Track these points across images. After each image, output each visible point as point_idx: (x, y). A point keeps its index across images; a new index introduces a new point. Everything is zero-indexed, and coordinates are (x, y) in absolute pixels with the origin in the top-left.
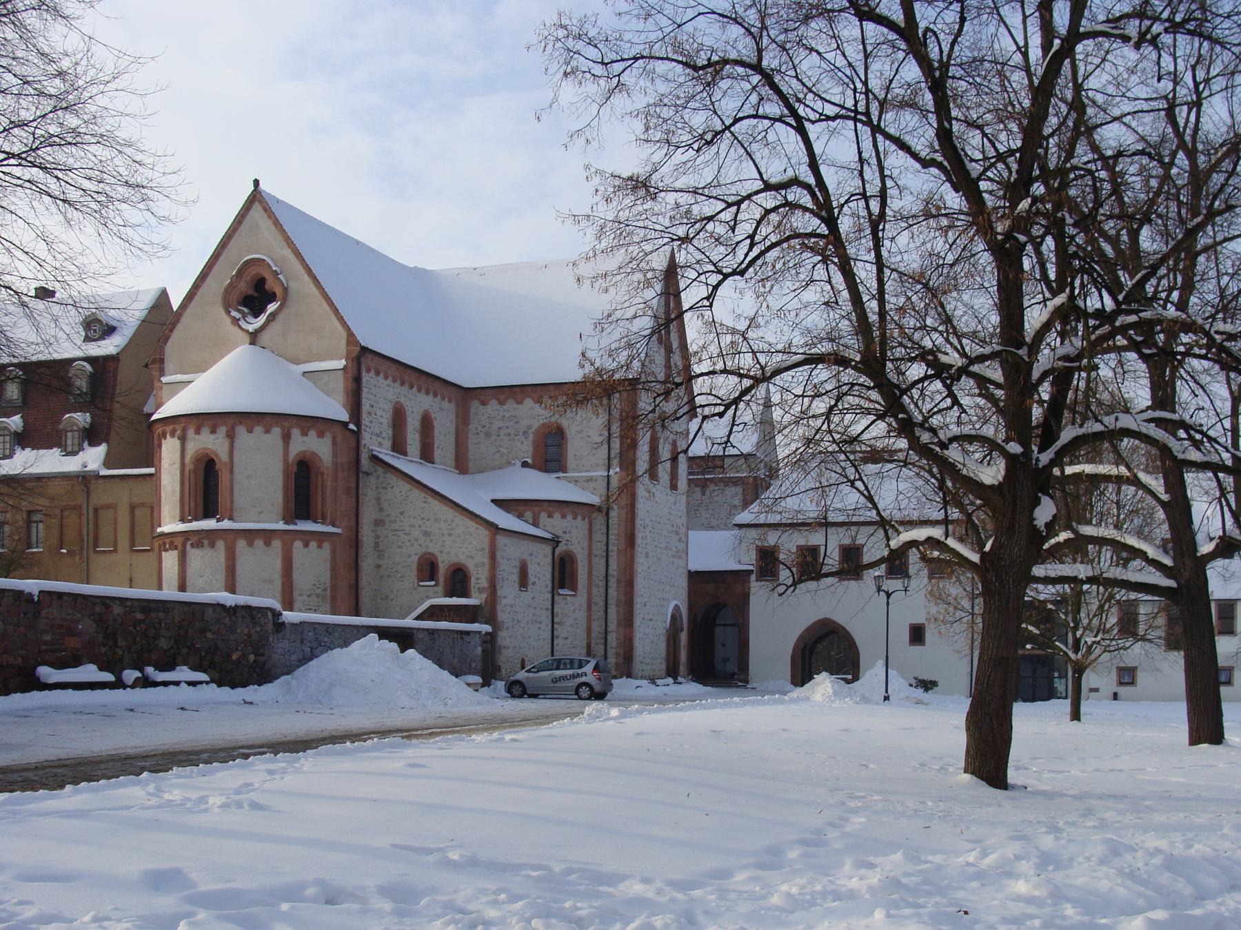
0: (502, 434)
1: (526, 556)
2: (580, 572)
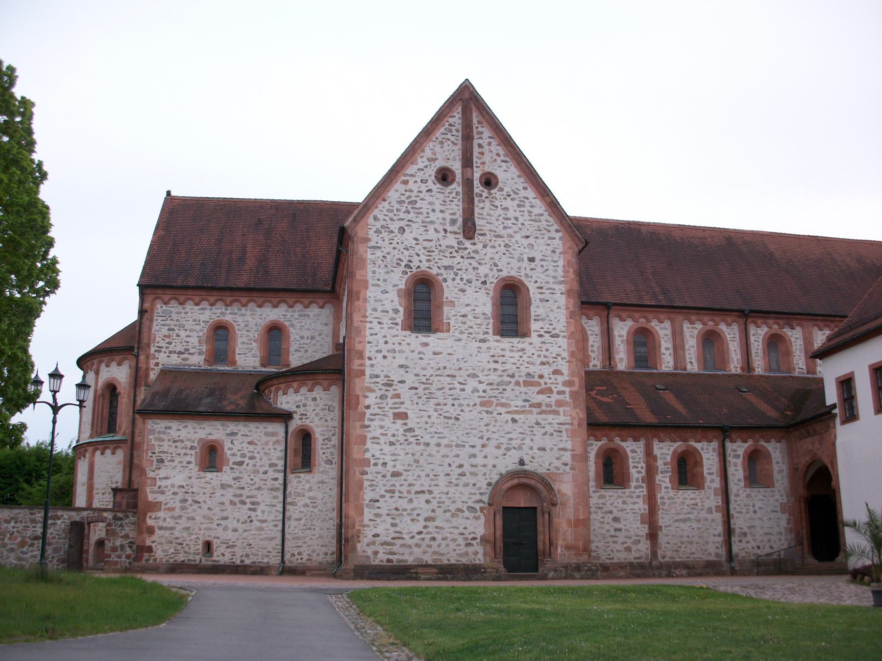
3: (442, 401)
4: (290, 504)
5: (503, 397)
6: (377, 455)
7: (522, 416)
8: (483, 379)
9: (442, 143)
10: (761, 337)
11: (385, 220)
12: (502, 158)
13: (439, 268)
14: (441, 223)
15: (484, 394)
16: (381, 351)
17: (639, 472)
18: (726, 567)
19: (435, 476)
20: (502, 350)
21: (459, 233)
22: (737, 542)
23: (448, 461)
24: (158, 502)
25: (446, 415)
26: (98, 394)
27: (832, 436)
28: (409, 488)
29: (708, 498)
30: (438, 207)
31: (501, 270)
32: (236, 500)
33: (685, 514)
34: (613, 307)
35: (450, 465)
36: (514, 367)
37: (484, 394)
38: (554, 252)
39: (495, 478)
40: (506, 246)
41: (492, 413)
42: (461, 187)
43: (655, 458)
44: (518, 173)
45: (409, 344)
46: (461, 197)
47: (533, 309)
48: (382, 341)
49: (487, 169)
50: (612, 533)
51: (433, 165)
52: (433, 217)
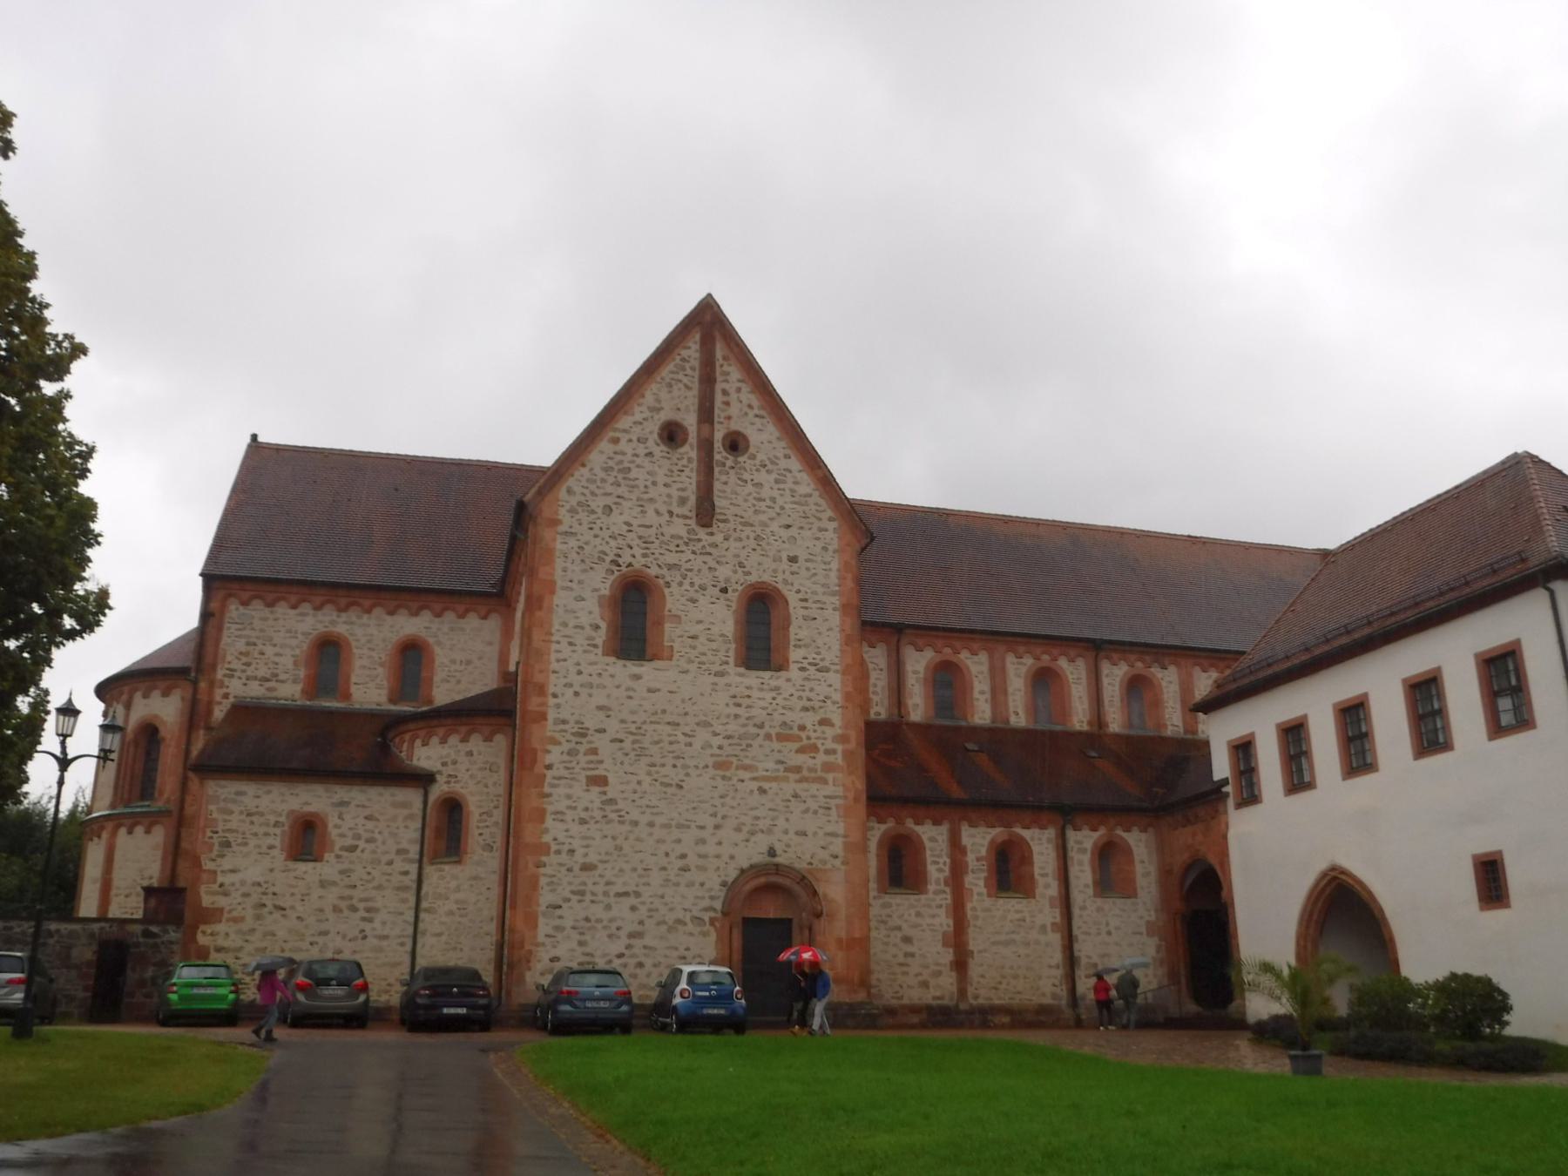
3: (658, 760)
5: (747, 757)
6: (561, 837)
7: (774, 785)
8: (719, 729)
9: (670, 385)
10: (1118, 679)
11: (583, 494)
12: (756, 411)
13: (659, 566)
14: (665, 502)
15: (718, 752)
16: (571, 685)
17: (940, 870)
18: (1068, 1013)
19: (645, 870)
20: (747, 688)
21: (690, 518)
22: (1083, 977)
23: (663, 848)
24: (217, 909)
25: (665, 780)
26: (127, 739)
27: (1223, 826)
28: (607, 888)
29: (1041, 911)
30: (661, 479)
31: (749, 573)
32: (343, 904)
33: (1007, 933)
34: (908, 631)
35: (667, 854)
36: (765, 713)
37: (718, 752)
38: (825, 549)
39: (732, 874)
40: (757, 538)
41: (730, 779)
42: (695, 452)
43: (963, 851)
44: (777, 434)
45: (612, 676)
46: (694, 465)
47: (792, 630)
48: (573, 670)
49: (735, 426)
50: (901, 959)
51: (656, 417)
52: (653, 493)
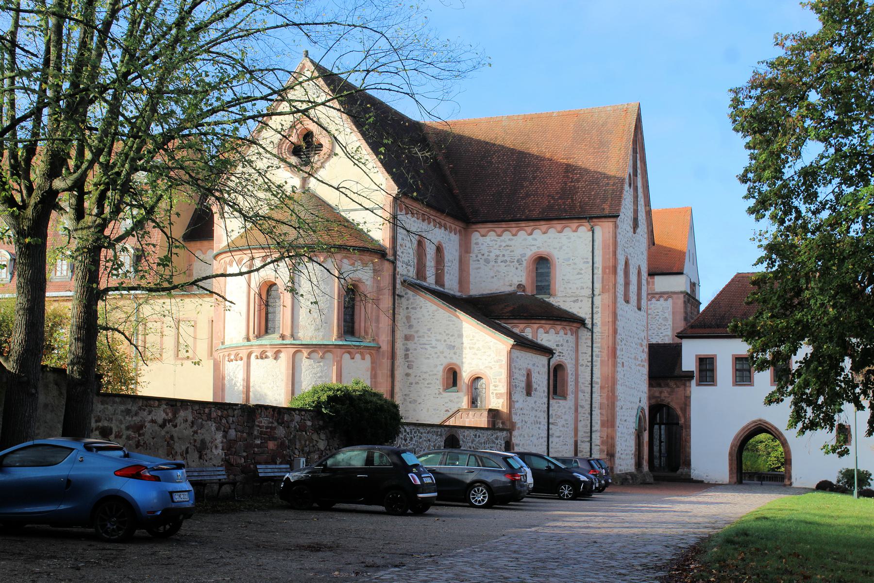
0: (499, 261)
1: (530, 367)
2: (569, 380)
4: (552, 424)
